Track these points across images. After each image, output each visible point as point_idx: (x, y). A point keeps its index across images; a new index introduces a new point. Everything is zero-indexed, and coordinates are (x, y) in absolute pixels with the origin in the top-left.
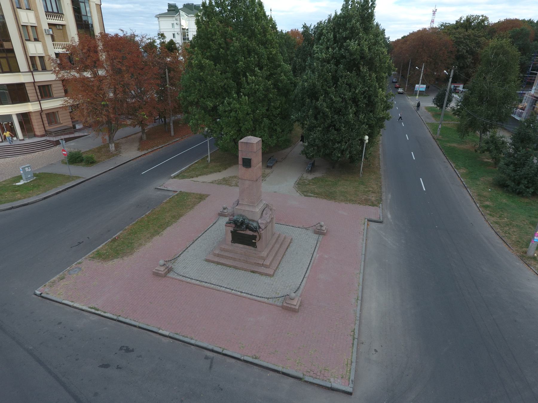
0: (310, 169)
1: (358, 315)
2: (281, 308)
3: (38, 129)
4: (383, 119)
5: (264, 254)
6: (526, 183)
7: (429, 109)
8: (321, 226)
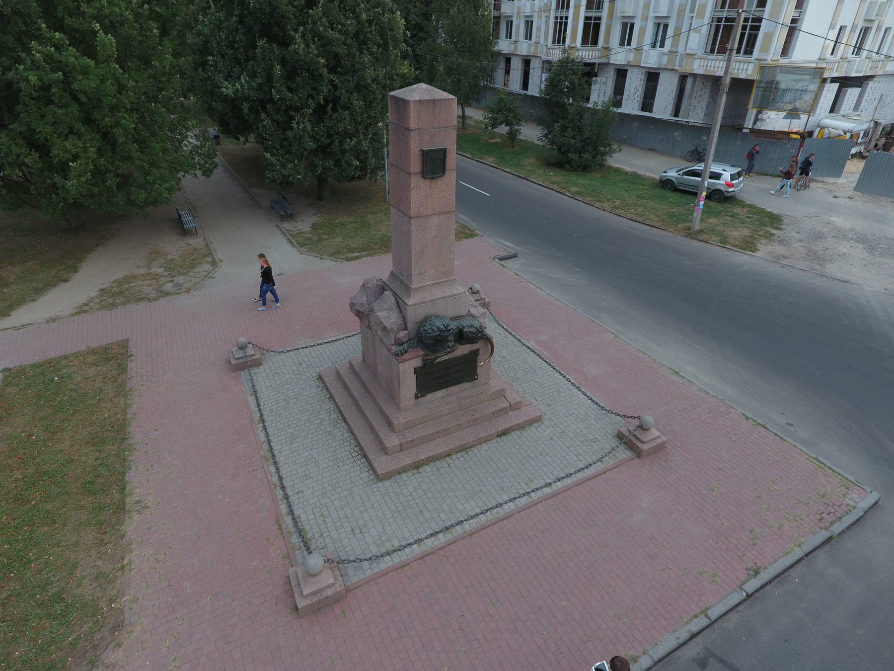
2: (637, 460)
5: (495, 384)
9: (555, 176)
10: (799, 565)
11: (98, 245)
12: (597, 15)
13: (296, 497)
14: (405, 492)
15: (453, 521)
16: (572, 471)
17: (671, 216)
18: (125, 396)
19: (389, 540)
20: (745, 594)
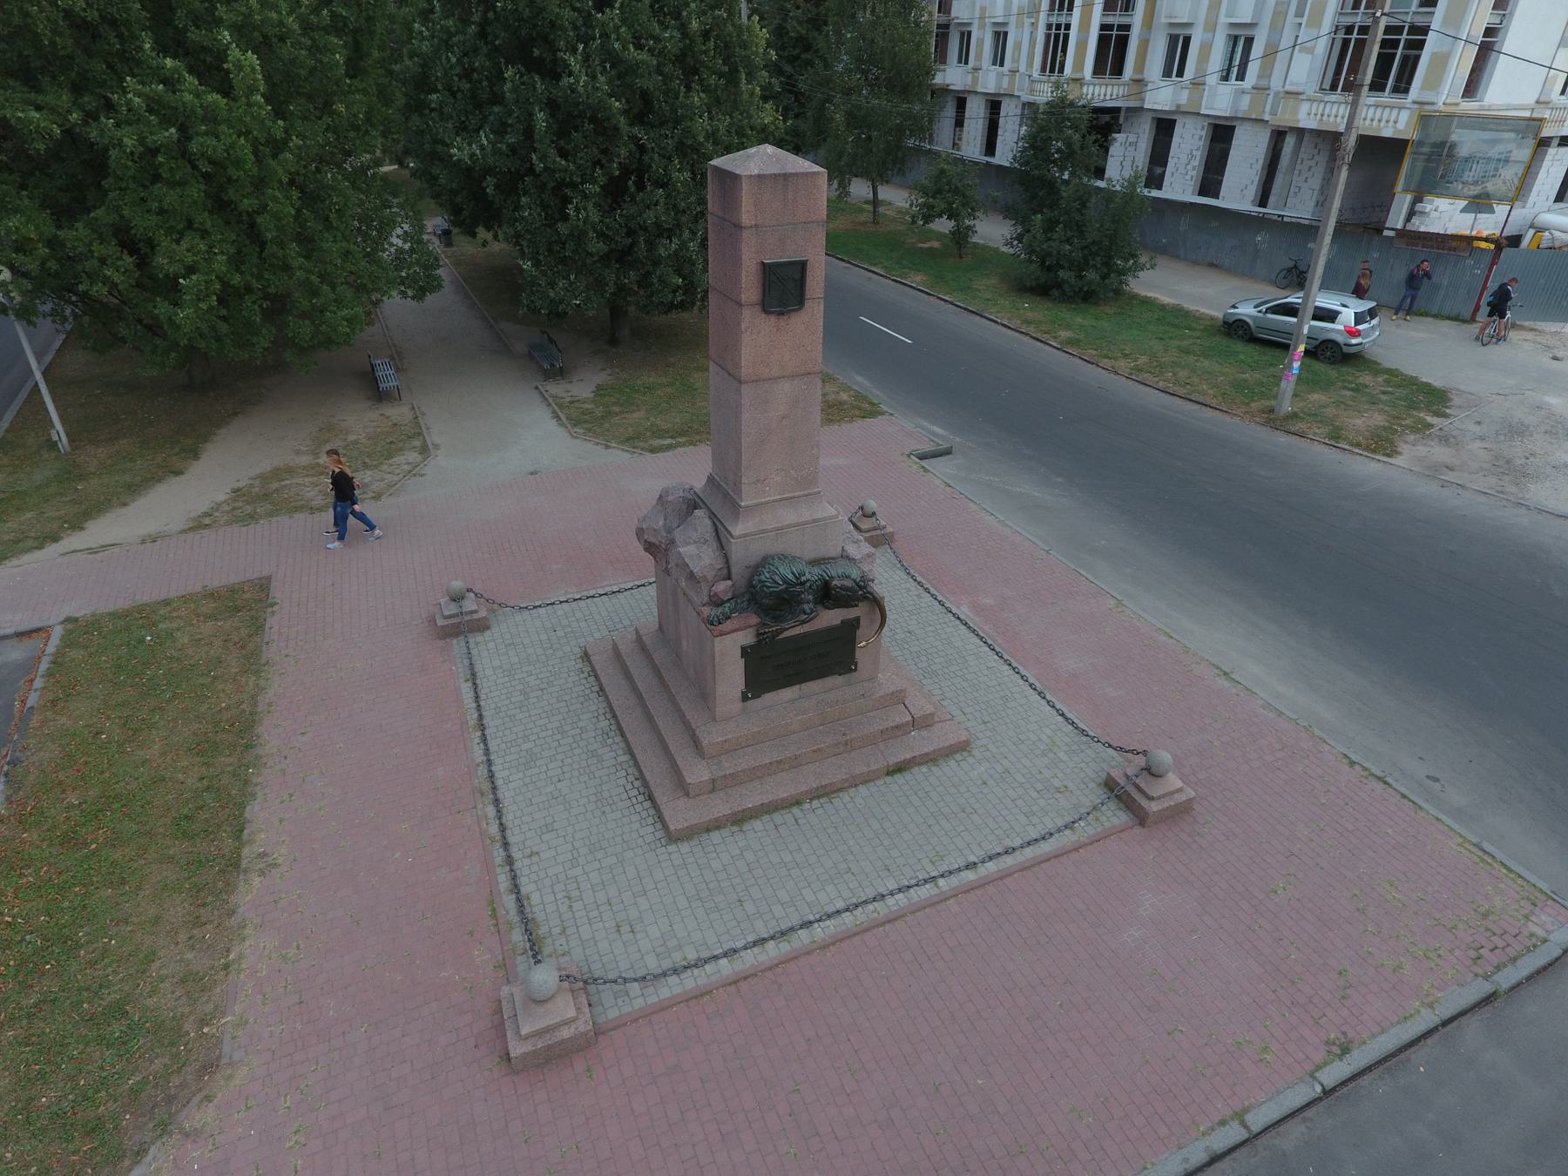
2: (1138, 830)
5: (887, 681)
9: (1030, 308)
10: (1429, 1041)
11: (236, 414)
12: (1124, 20)
13: (527, 861)
14: (716, 864)
15: (795, 920)
16: (1017, 842)
17: (1239, 386)
18: (257, 673)
19: (680, 947)
20: (1318, 1089)
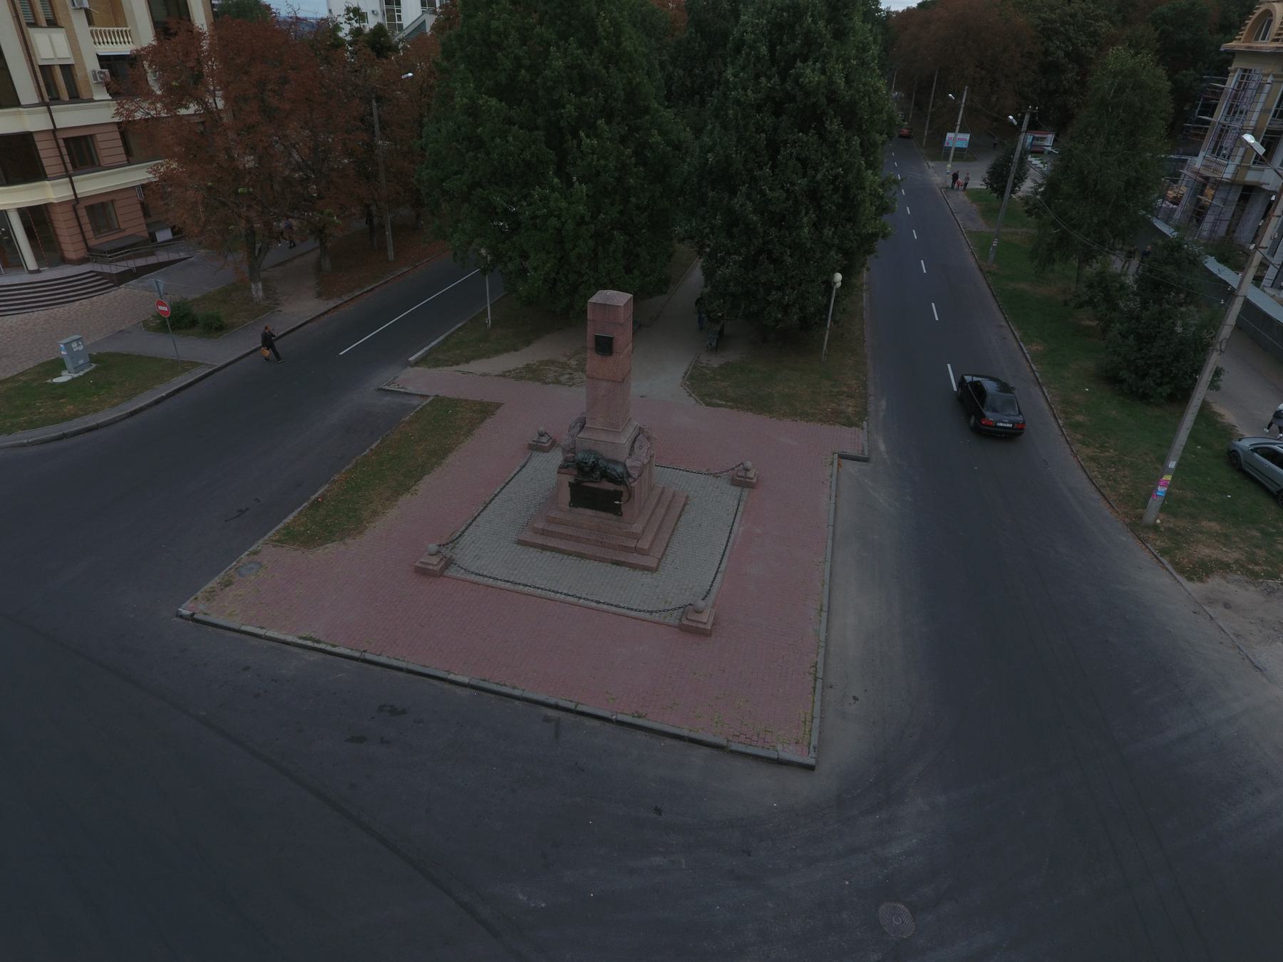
0: (714, 344)
1: (822, 638)
3: (71, 247)
4: (874, 236)
5: (637, 527)
6: (1159, 375)
7: (975, 196)
8: (747, 470)
